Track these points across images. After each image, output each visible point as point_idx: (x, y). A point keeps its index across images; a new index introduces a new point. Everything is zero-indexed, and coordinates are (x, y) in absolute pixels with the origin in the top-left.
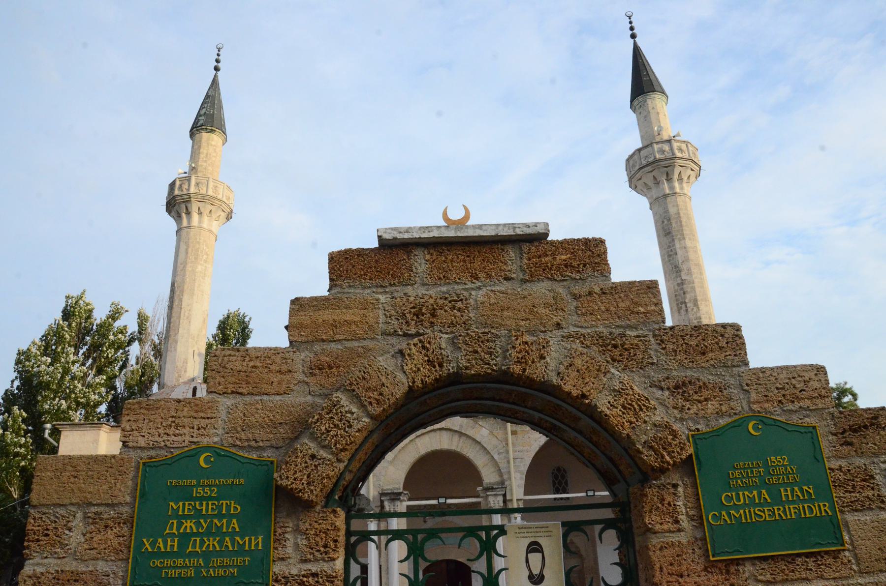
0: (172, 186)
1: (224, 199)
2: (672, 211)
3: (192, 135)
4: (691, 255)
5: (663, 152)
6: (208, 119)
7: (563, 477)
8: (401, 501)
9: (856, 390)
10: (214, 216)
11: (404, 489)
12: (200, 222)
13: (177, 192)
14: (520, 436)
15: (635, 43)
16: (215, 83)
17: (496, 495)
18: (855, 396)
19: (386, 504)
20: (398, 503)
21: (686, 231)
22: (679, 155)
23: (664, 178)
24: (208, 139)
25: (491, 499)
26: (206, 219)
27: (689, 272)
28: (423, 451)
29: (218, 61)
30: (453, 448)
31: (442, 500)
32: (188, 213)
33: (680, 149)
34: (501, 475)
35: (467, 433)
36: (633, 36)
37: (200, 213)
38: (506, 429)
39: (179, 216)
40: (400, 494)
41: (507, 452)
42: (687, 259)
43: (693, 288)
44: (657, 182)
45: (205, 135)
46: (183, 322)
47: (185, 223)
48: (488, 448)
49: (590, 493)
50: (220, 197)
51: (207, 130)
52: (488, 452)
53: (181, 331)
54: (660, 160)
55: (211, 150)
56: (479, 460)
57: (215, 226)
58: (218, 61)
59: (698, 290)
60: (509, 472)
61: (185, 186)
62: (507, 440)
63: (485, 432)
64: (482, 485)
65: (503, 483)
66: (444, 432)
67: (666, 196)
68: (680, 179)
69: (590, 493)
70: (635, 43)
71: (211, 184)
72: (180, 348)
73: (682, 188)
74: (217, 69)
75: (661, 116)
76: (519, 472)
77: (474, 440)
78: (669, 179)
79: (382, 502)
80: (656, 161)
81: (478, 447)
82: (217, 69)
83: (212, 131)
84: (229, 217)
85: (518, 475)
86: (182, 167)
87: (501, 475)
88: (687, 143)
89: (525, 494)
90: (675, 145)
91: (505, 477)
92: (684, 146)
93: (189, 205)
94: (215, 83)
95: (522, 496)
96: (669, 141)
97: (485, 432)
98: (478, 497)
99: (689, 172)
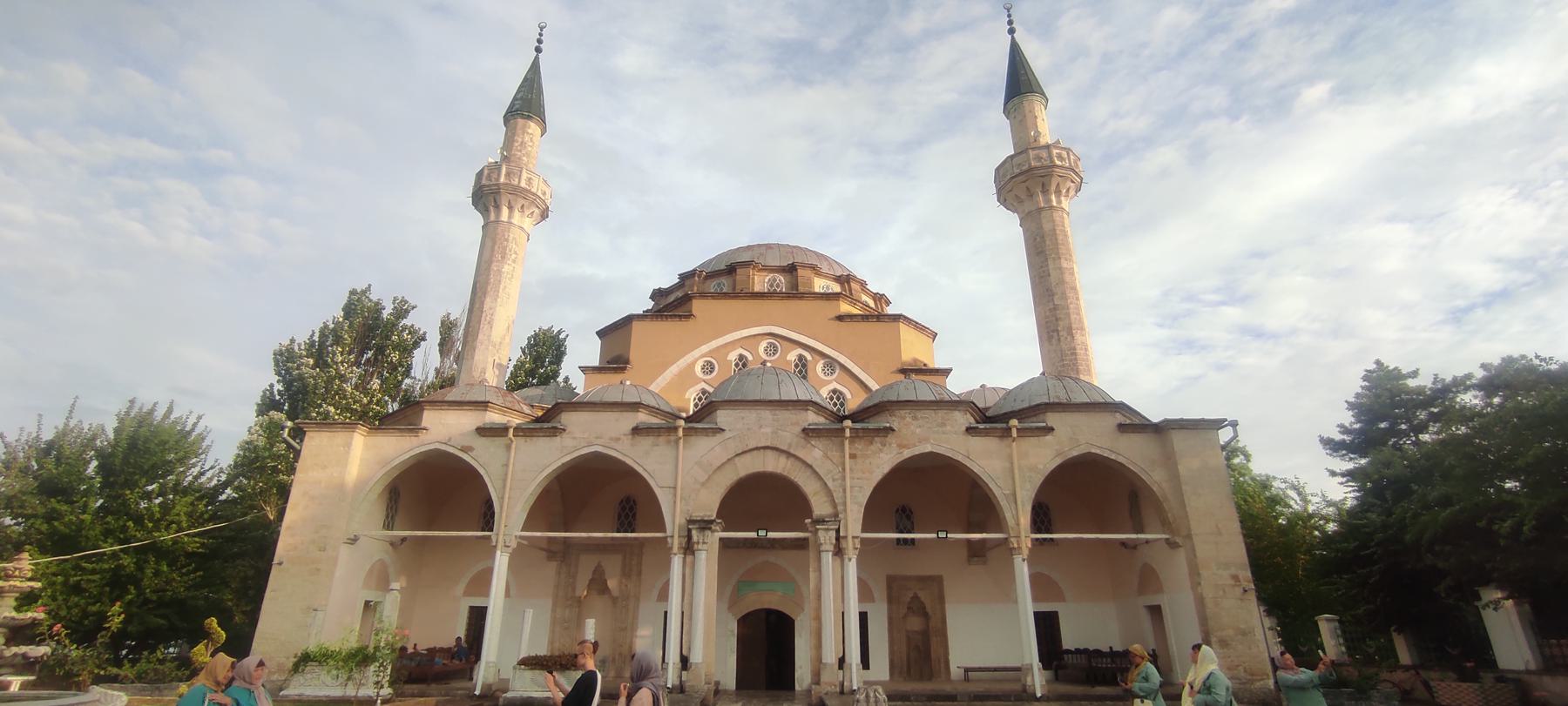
0: (480, 175)
2: (1047, 226)
3: (507, 120)
4: (1067, 278)
5: (1039, 158)
6: (527, 104)
9: (1250, 450)
10: (527, 212)
11: (719, 515)
12: (510, 217)
13: (484, 182)
14: (859, 460)
16: (535, 66)
18: (1247, 457)
19: (694, 532)
20: (708, 533)
21: (1062, 250)
22: (1058, 163)
23: (1039, 190)
24: (524, 126)
25: (821, 534)
26: (517, 214)
27: (1064, 297)
28: (743, 473)
29: (540, 41)
30: (779, 471)
31: (762, 533)
32: (498, 207)
33: (1060, 157)
34: (835, 506)
36: (1012, 31)
37: (511, 208)
38: (843, 451)
39: (487, 210)
40: (712, 522)
41: (844, 478)
42: (1062, 282)
43: (1068, 315)
44: (1031, 195)
45: (520, 121)
46: (484, 327)
47: (492, 217)
49: (942, 535)
51: (523, 117)
52: (820, 478)
53: (480, 336)
54: (1036, 168)
55: (527, 138)
56: (809, 486)
57: (527, 223)
58: (540, 41)
59: (1073, 317)
60: (845, 504)
61: (494, 176)
63: (818, 453)
64: (810, 516)
65: (836, 515)
66: (769, 452)
67: (1040, 210)
68: (1058, 192)
69: (942, 535)
71: (525, 175)
72: (478, 356)
73: (1059, 202)
74: (538, 50)
75: (1039, 121)
77: (804, 462)
78: (1045, 191)
79: (689, 531)
80: (1031, 169)
81: (809, 472)
82: (538, 50)
83: (529, 118)
84: (544, 215)
86: (494, 157)
87: (835, 506)
88: (1068, 150)
89: (864, 530)
90: (1055, 151)
91: (840, 508)
92: (1064, 154)
94: (535, 66)
96: (1048, 147)
97: (818, 453)
98: (806, 530)
99: (1069, 184)
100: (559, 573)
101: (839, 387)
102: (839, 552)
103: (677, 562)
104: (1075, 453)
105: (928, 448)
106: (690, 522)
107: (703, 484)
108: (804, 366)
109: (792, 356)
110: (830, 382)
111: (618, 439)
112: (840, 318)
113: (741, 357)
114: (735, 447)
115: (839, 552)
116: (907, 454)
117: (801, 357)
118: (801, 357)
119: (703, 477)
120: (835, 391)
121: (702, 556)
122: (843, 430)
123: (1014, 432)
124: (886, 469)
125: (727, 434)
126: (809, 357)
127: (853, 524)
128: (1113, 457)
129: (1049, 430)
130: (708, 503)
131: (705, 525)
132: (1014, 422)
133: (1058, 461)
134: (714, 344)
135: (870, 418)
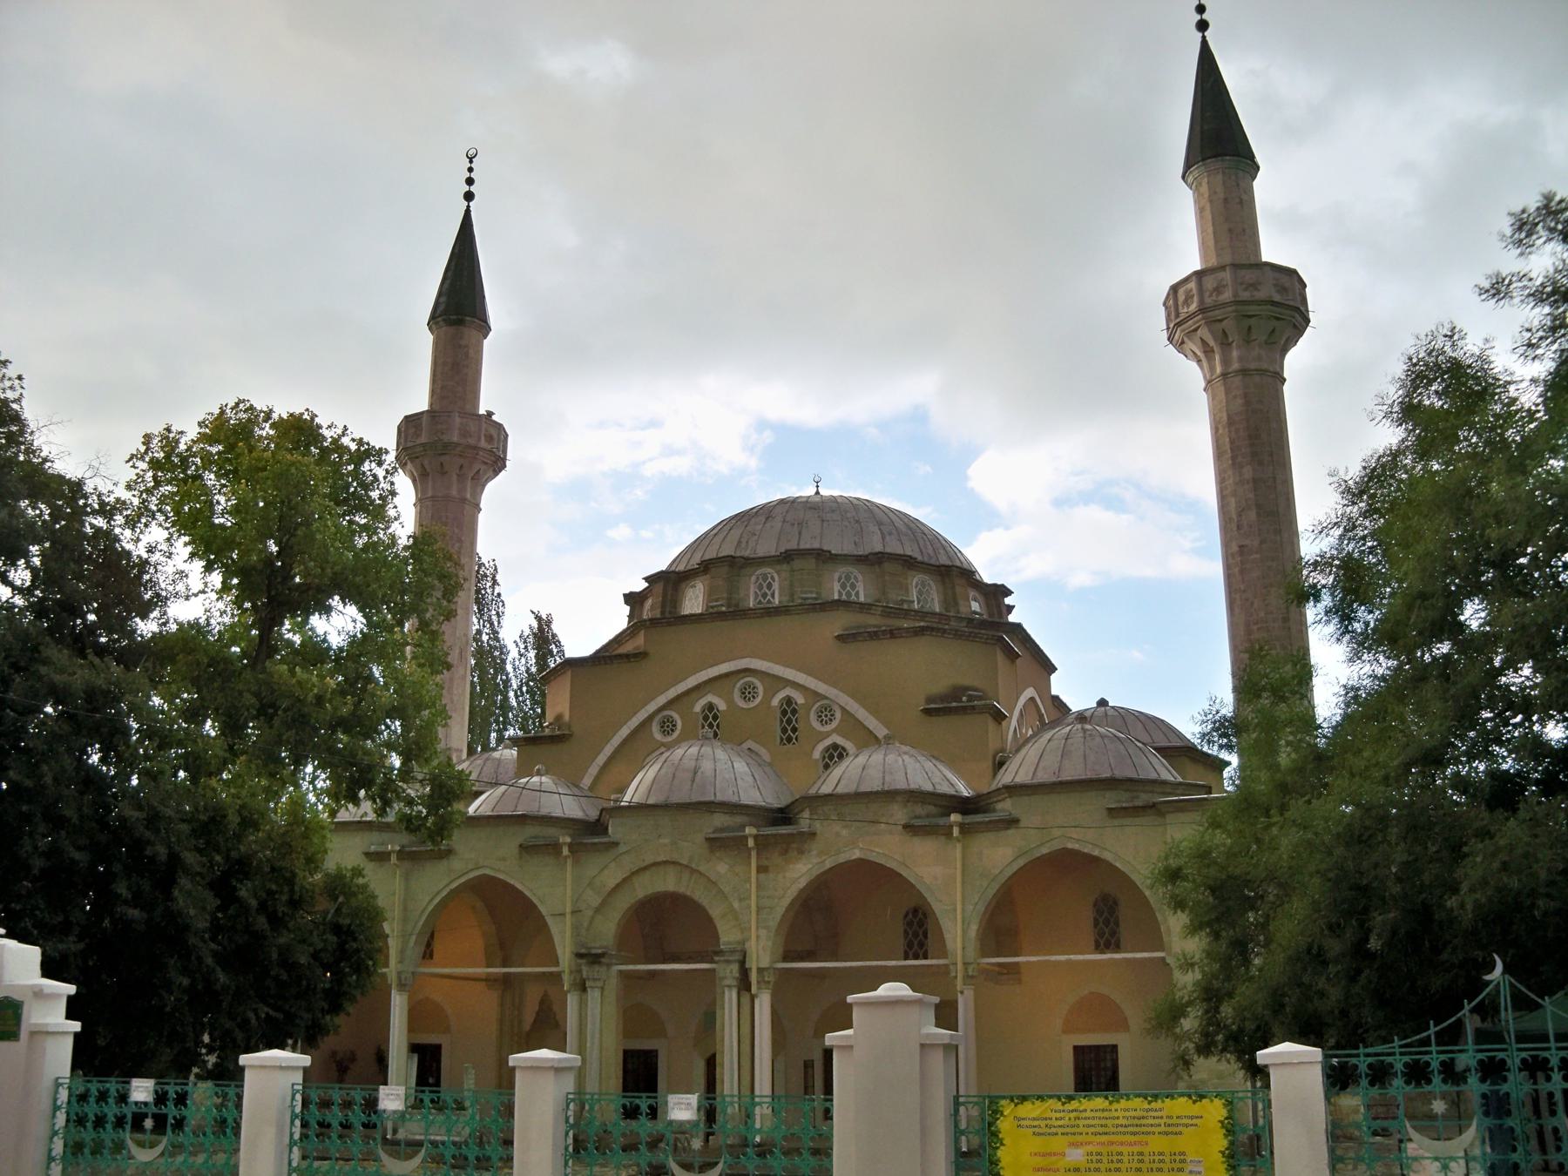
1: (483, 444)
7: (921, 924)
8: (609, 966)
15: (1204, 43)
17: (728, 962)
29: (470, 181)
30: (682, 890)
35: (701, 869)
48: (726, 890)
50: (472, 441)
58: (470, 181)
62: (749, 880)
70: (1204, 43)
74: (469, 196)
76: (767, 928)
82: (469, 196)
85: (763, 932)
93: (426, 463)
95: (765, 963)
98: (712, 961)
100: (502, 1005)
101: (840, 741)
102: (744, 984)
103: (572, 1001)
104: (1045, 850)
105: (857, 854)
106: (579, 956)
107: (597, 910)
108: (794, 712)
109: (775, 702)
110: (828, 734)
111: (504, 859)
112: (839, 638)
113: (711, 707)
114: (629, 864)
115: (744, 984)
116: (828, 865)
117: (789, 701)
118: (789, 701)
119: (596, 901)
120: (835, 746)
121: (594, 996)
122: (746, 838)
123: (956, 831)
124: (802, 883)
125: (622, 848)
126: (800, 699)
127: (762, 952)
128: (1096, 853)
129: (1012, 822)
130: (606, 931)
131: (594, 959)
132: (955, 817)
133: (1021, 862)
134: (672, 693)
135: (781, 823)
